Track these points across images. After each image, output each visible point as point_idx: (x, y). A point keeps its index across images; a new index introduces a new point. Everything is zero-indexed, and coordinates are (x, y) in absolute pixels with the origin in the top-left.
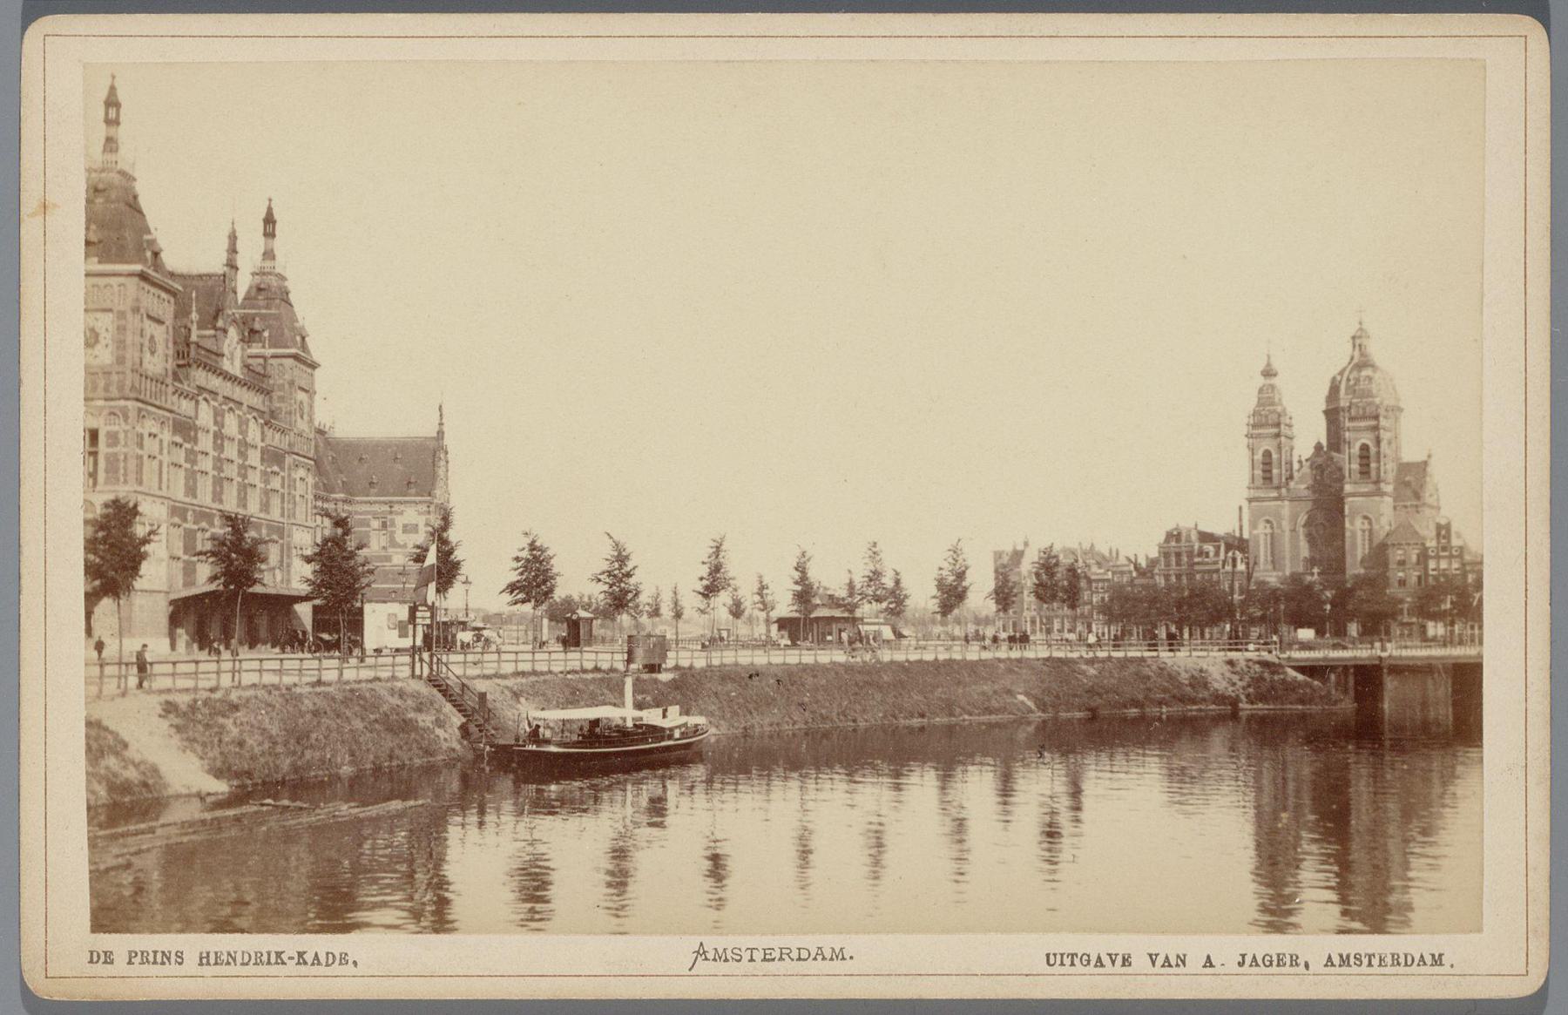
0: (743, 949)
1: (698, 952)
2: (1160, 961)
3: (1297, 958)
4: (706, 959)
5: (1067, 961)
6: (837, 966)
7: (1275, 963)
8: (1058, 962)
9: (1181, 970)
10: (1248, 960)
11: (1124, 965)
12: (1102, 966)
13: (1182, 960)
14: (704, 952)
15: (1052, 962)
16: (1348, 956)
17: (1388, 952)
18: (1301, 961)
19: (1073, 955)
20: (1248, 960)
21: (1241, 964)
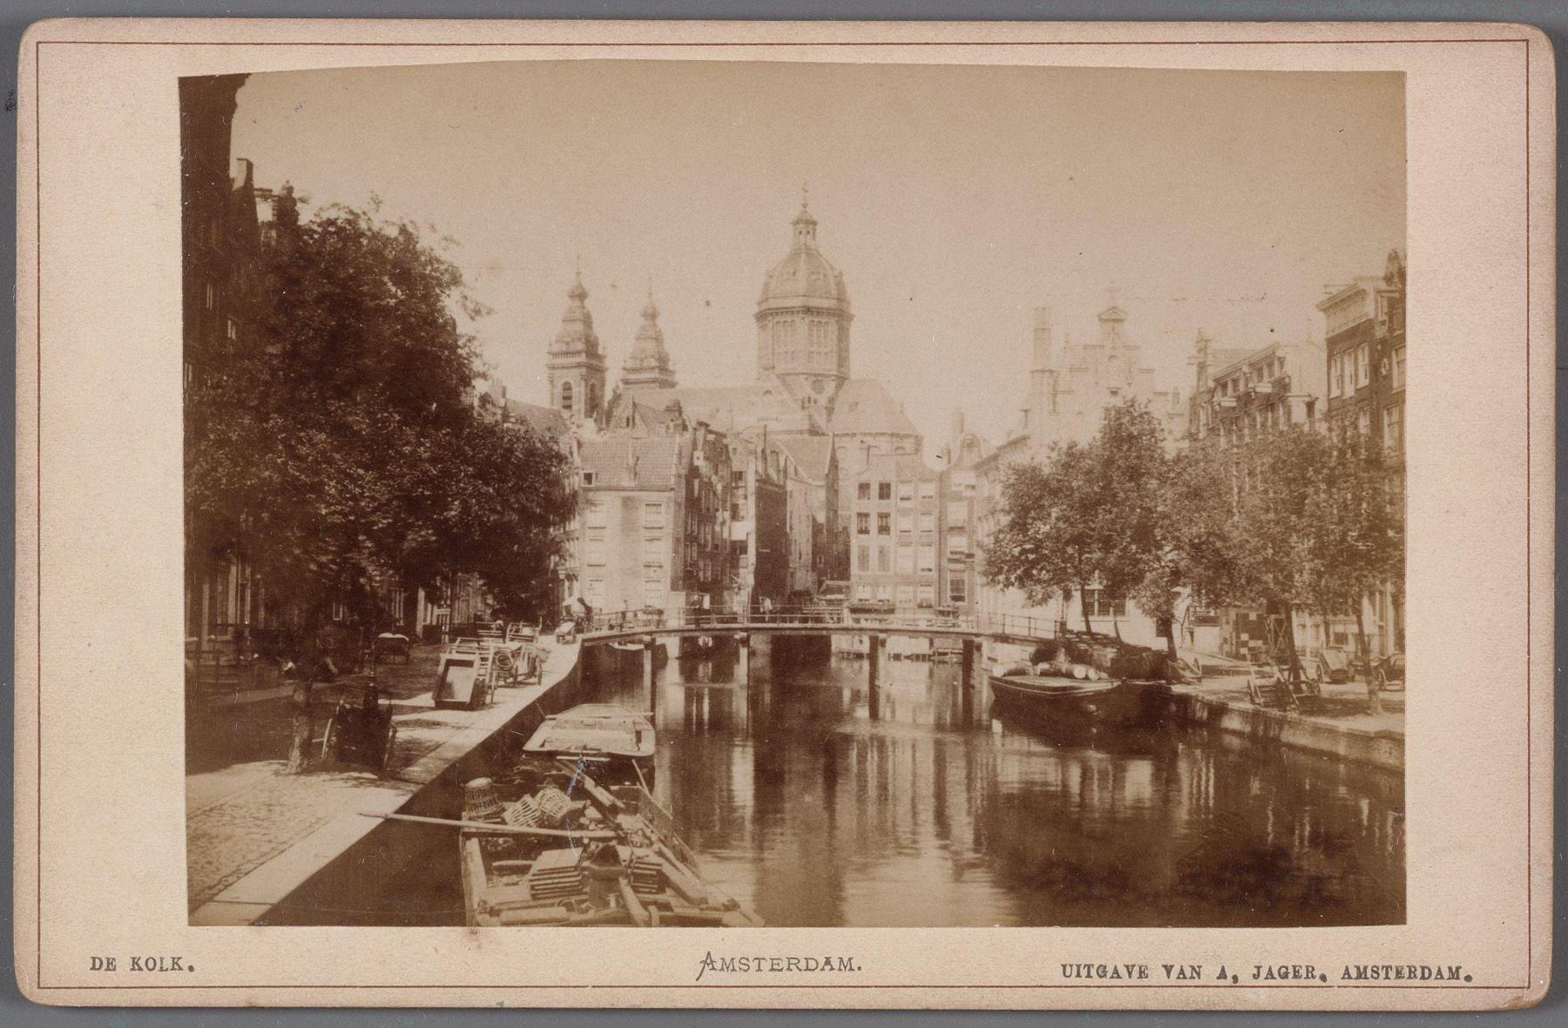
0: (751, 959)
1: (705, 962)
2: (1175, 972)
3: (1313, 969)
4: (713, 969)
5: (1084, 972)
6: (845, 977)
7: (1291, 975)
8: (1075, 973)
9: (1196, 982)
10: (1264, 973)
11: (1140, 977)
12: (1119, 977)
13: (1197, 971)
14: (712, 962)
15: (1068, 974)
16: (1365, 968)
17: (1404, 963)
18: (1317, 973)
19: (1089, 967)
20: (1264, 973)
21: (1256, 976)
